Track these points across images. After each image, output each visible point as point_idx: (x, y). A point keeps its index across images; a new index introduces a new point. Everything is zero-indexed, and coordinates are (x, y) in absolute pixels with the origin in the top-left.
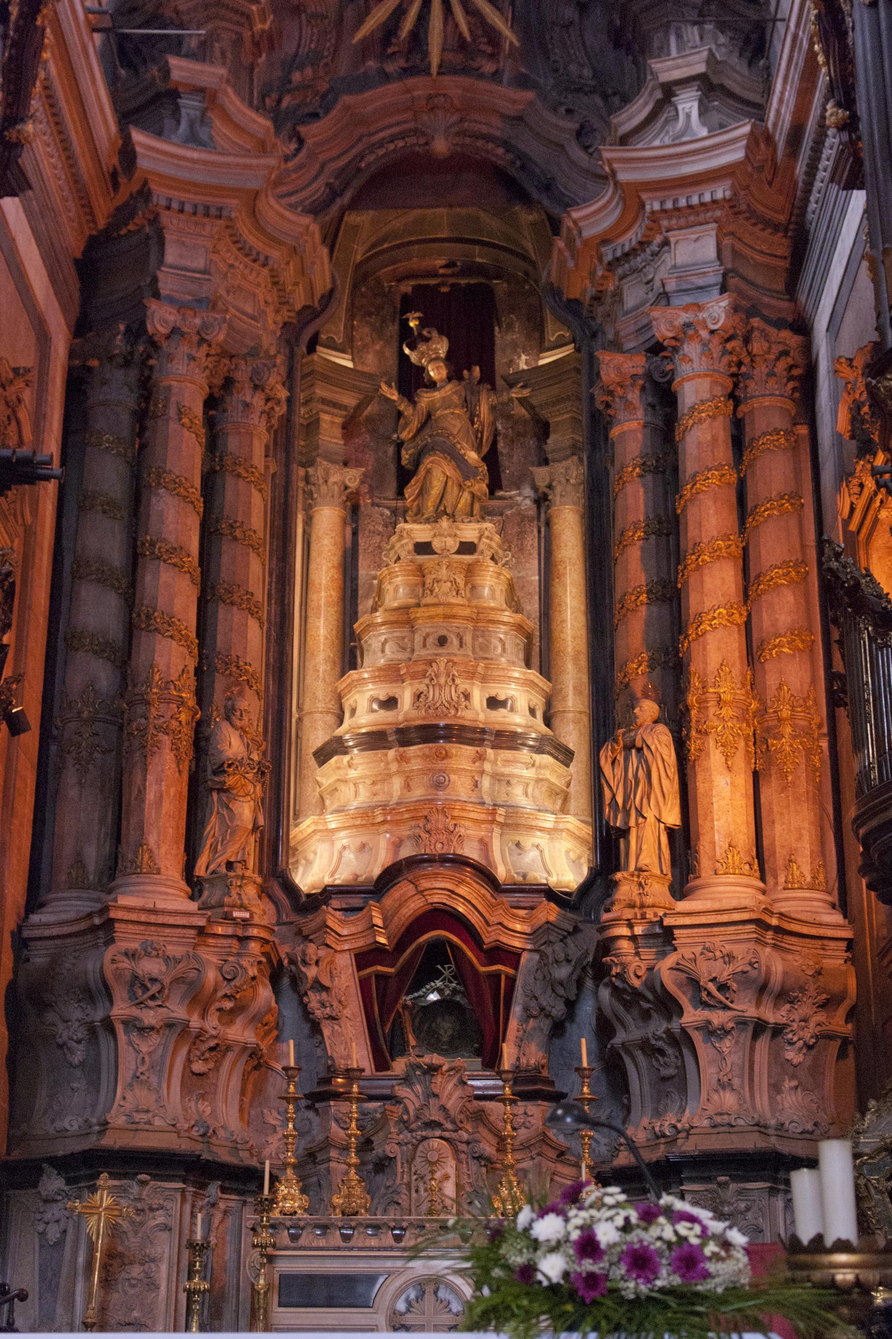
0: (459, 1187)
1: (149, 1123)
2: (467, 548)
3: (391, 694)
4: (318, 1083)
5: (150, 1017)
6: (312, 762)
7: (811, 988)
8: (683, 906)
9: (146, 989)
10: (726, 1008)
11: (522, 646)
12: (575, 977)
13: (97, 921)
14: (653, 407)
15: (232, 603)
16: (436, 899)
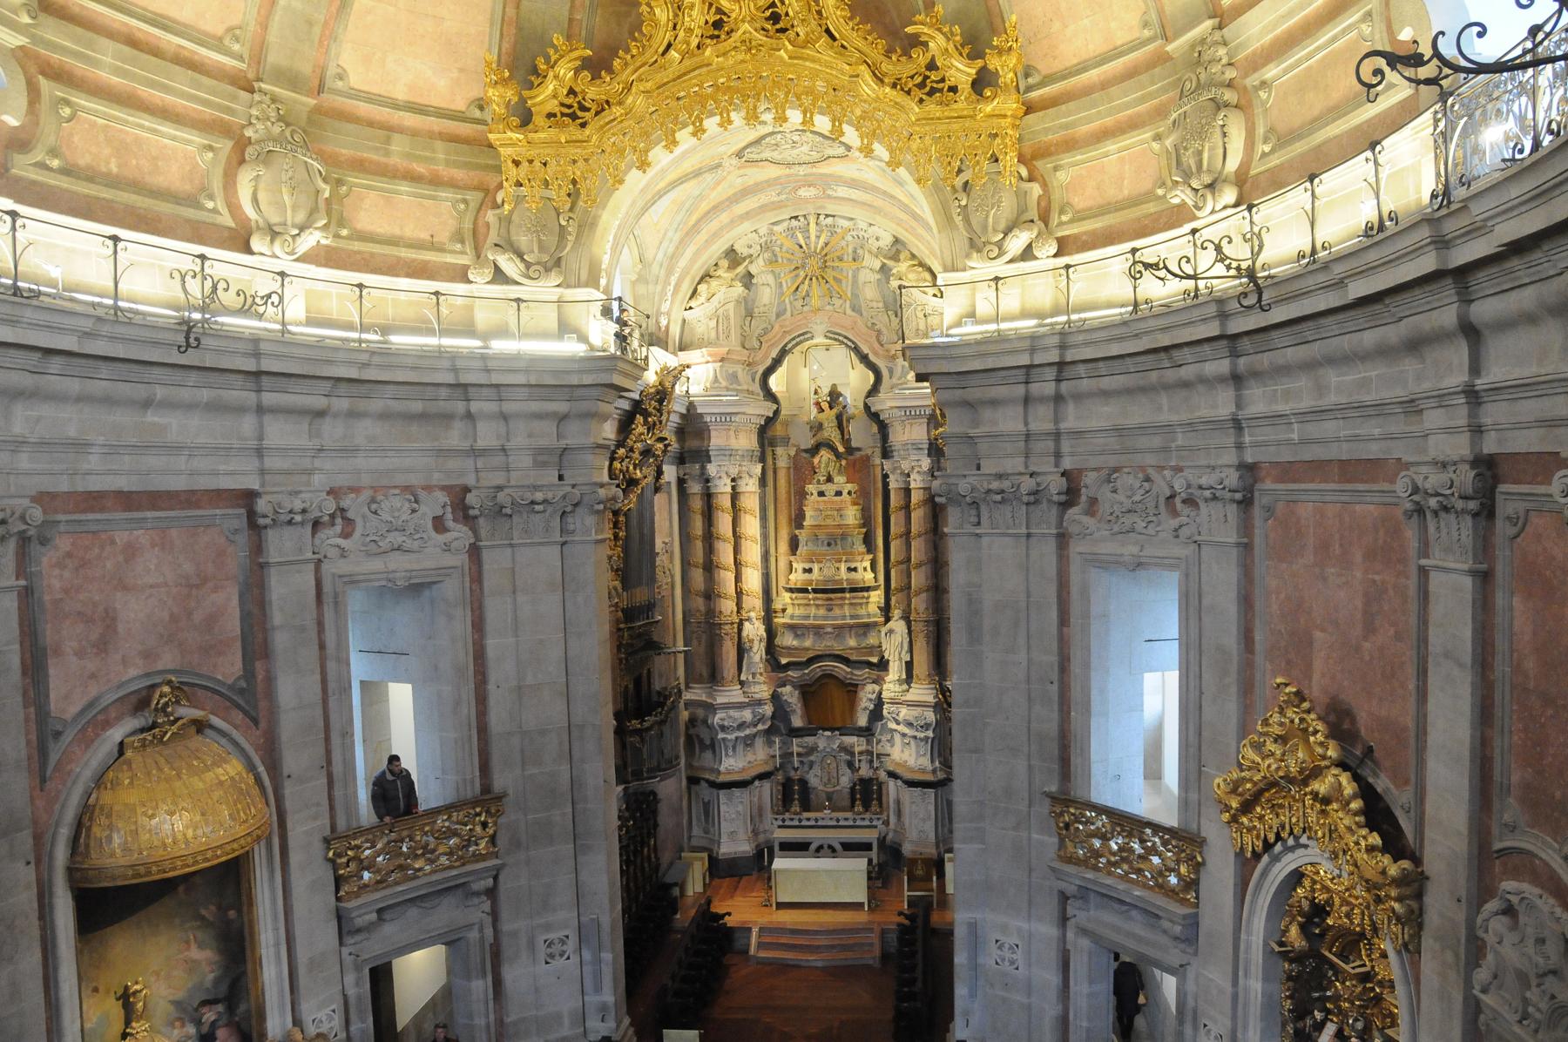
5: (729, 737)
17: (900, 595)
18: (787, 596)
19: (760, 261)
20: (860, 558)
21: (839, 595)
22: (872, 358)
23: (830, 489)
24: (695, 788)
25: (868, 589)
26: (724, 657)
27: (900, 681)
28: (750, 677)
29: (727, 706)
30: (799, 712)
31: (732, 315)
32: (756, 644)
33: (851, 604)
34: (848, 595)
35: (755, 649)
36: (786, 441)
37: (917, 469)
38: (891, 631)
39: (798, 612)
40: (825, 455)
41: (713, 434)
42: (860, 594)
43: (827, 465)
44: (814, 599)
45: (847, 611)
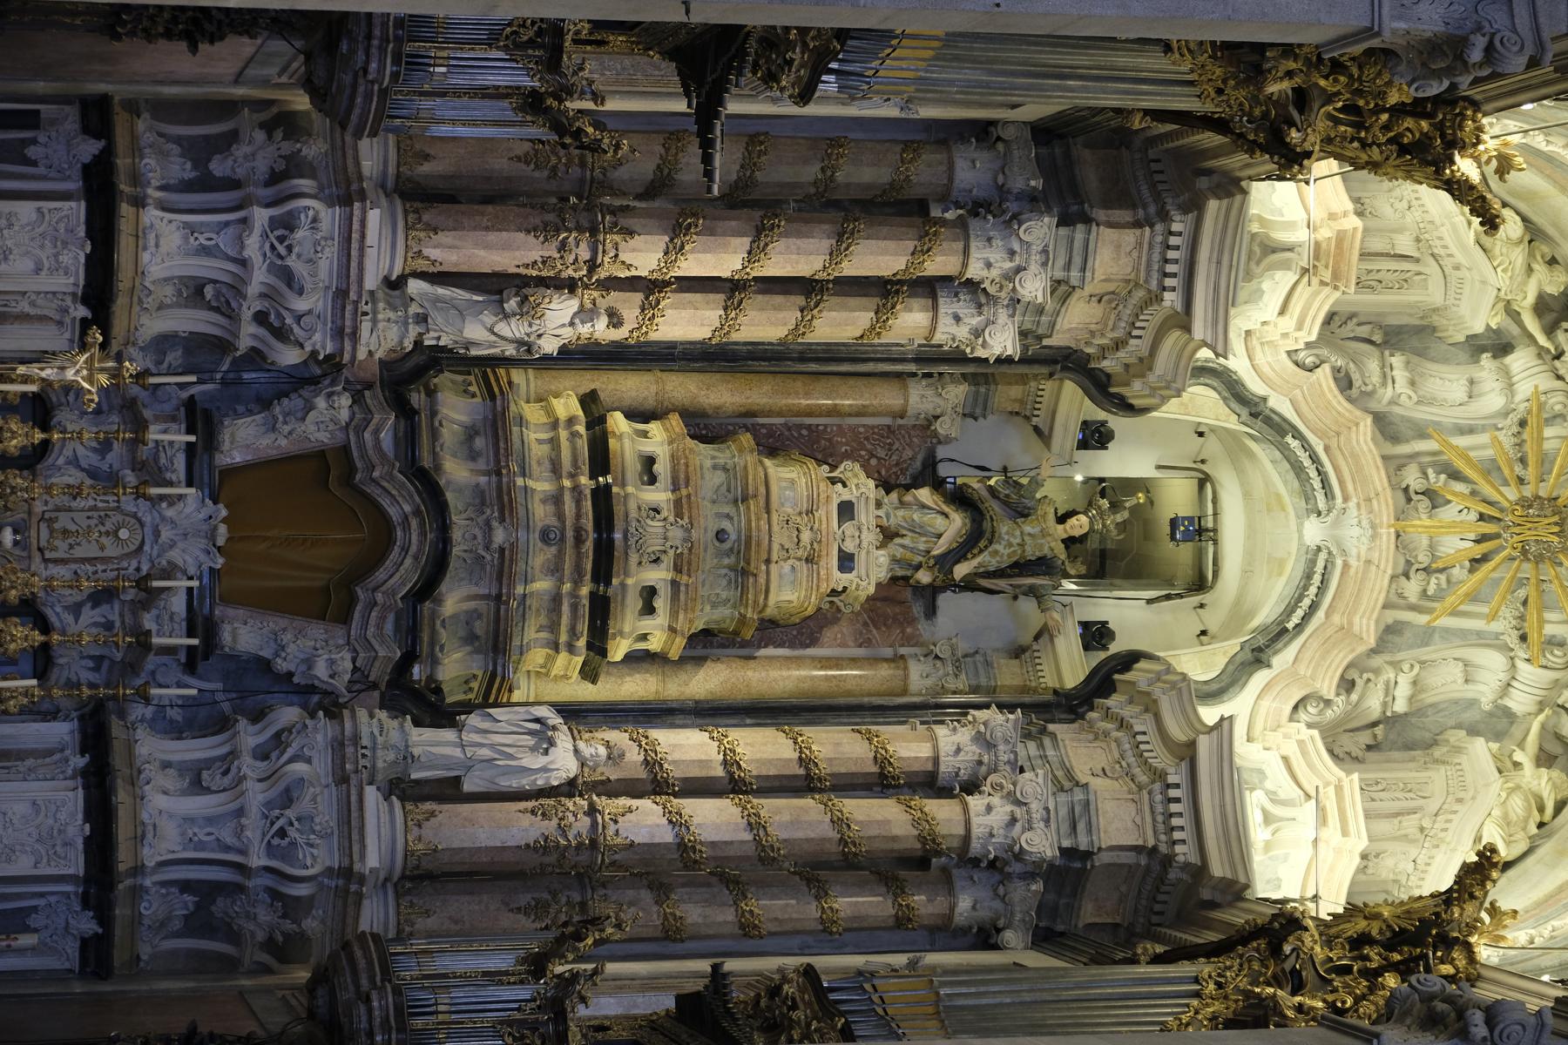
0: (91, 560)
1: (145, 248)
2: (846, 561)
3: (659, 478)
4: (206, 410)
6: (586, 387)
7: (288, 926)
8: (371, 795)
9: (281, 239)
10: (264, 835)
11: (723, 626)
12: (316, 683)
13: (354, 187)
14: (957, 774)
15: (725, 309)
16: (399, 533)
17: (634, 755)
18: (567, 406)
19: (1546, 382)
20: (681, 623)
21: (589, 566)
22: (1260, 678)
23: (862, 536)
24: (72, 114)
25: (598, 647)
26: (492, 237)
27: (408, 758)
28: (414, 309)
29: (350, 242)
30: (266, 441)
31: (1411, 296)
32: (515, 329)
33: (556, 599)
34: (585, 591)
35: (504, 329)
36: (973, 412)
37: (1018, 812)
38: (544, 739)
39: (534, 439)
40: (954, 524)
41: (1129, 237)
42: (583, 627)
43: (917, 530)
44: (576, 488)
45: (542, 585)
